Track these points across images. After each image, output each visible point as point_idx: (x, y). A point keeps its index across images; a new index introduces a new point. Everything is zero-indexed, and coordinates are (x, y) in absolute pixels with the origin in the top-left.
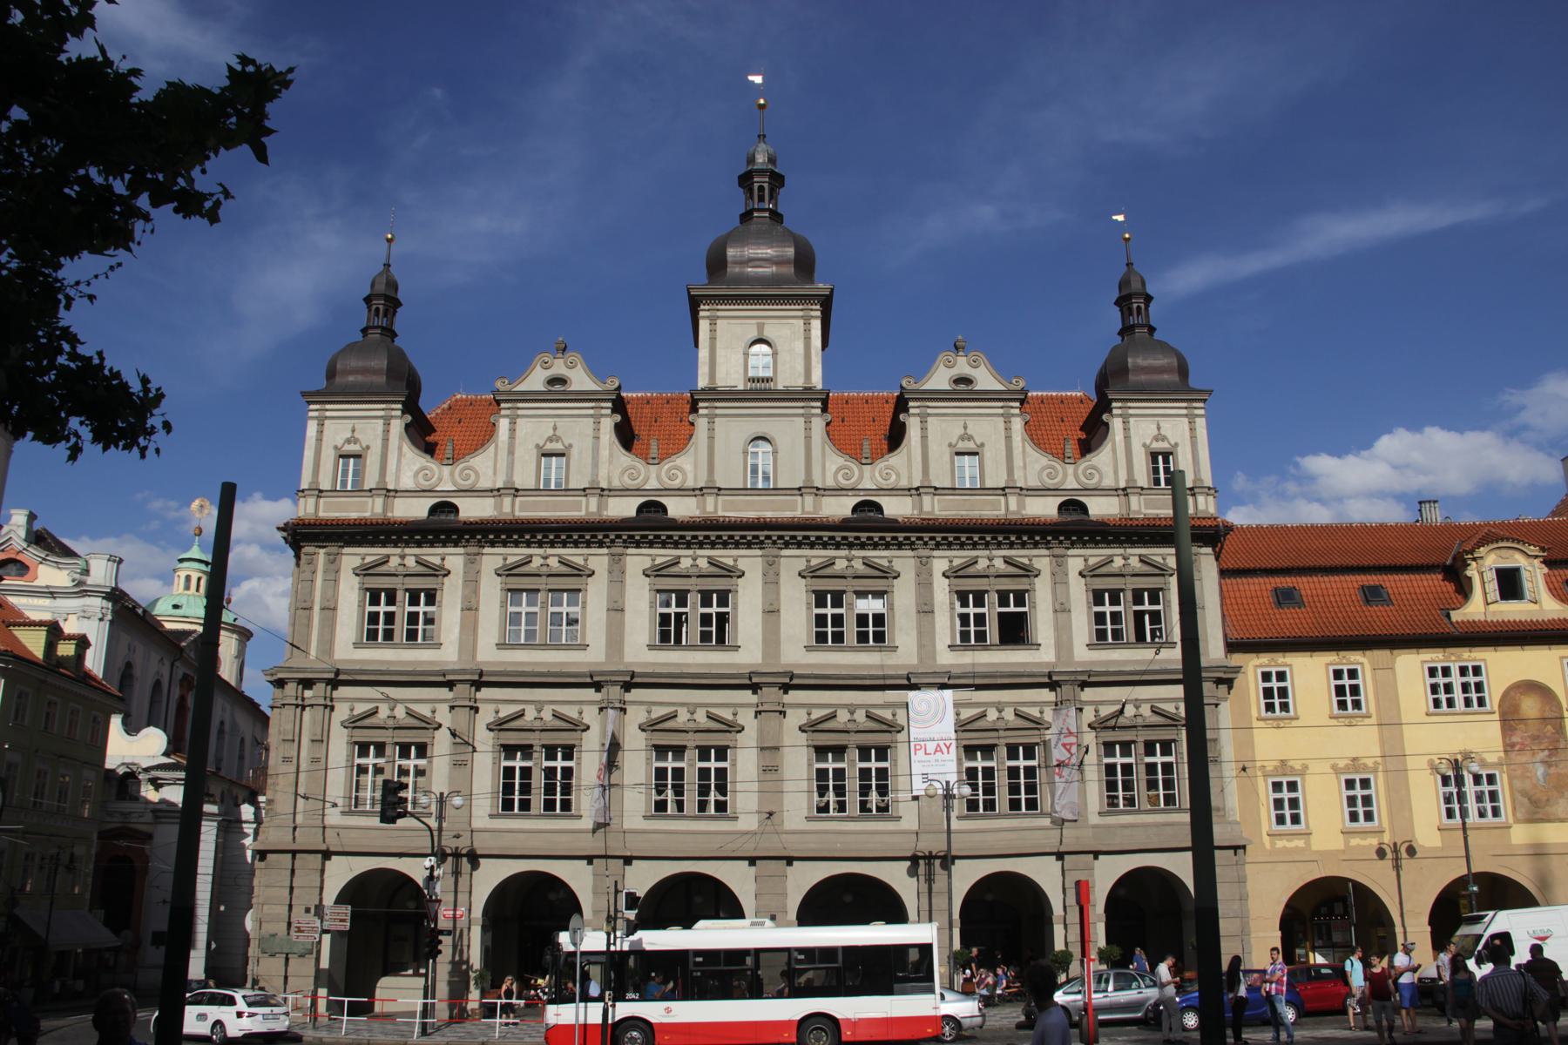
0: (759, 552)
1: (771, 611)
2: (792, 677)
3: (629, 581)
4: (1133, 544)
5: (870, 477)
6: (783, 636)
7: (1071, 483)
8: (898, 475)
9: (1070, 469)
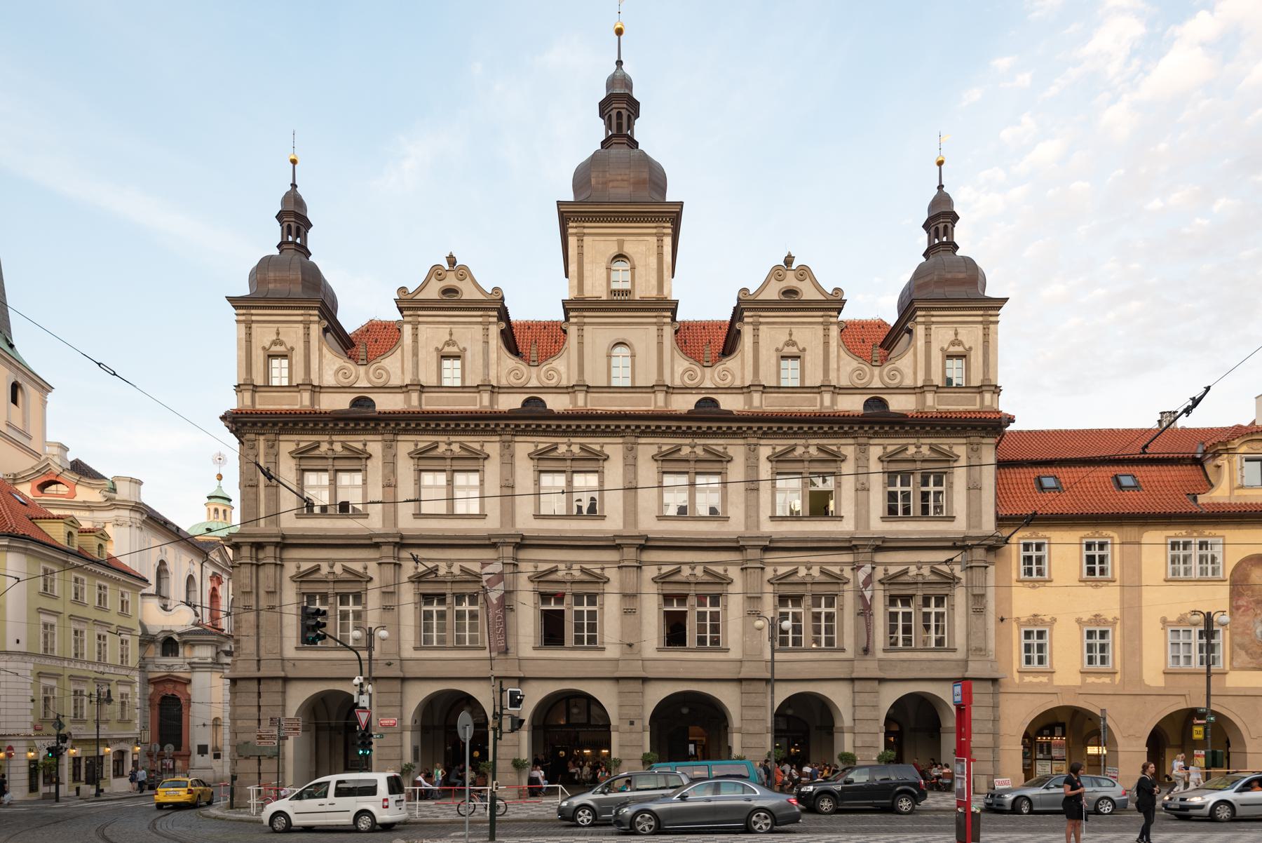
0: (620, 440)
1: (631, 489)
2: (647, 539)
4: (927, 435)
5: (710, 378)
6: (640, 509)
7: (876, 383)
8: (733, 376)
9: (877, 371)
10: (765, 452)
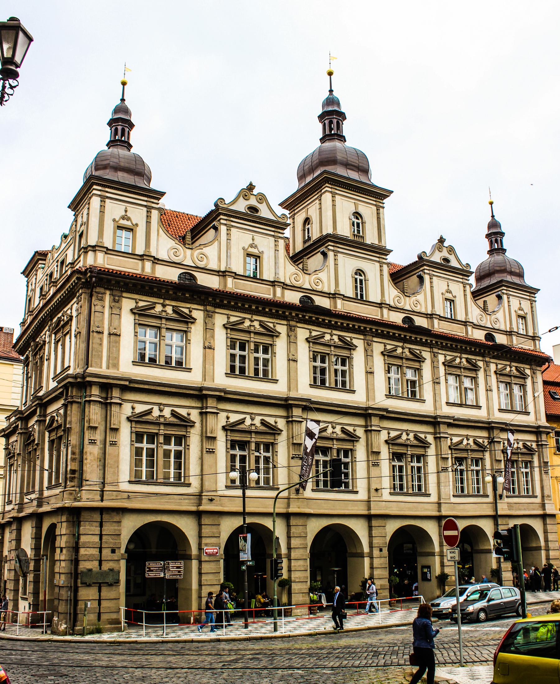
1: (370, 373)
3: (299, 343)
9: (488, 316)
10: (441, 358)
